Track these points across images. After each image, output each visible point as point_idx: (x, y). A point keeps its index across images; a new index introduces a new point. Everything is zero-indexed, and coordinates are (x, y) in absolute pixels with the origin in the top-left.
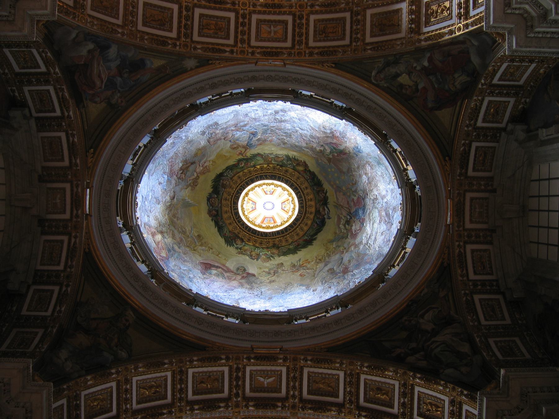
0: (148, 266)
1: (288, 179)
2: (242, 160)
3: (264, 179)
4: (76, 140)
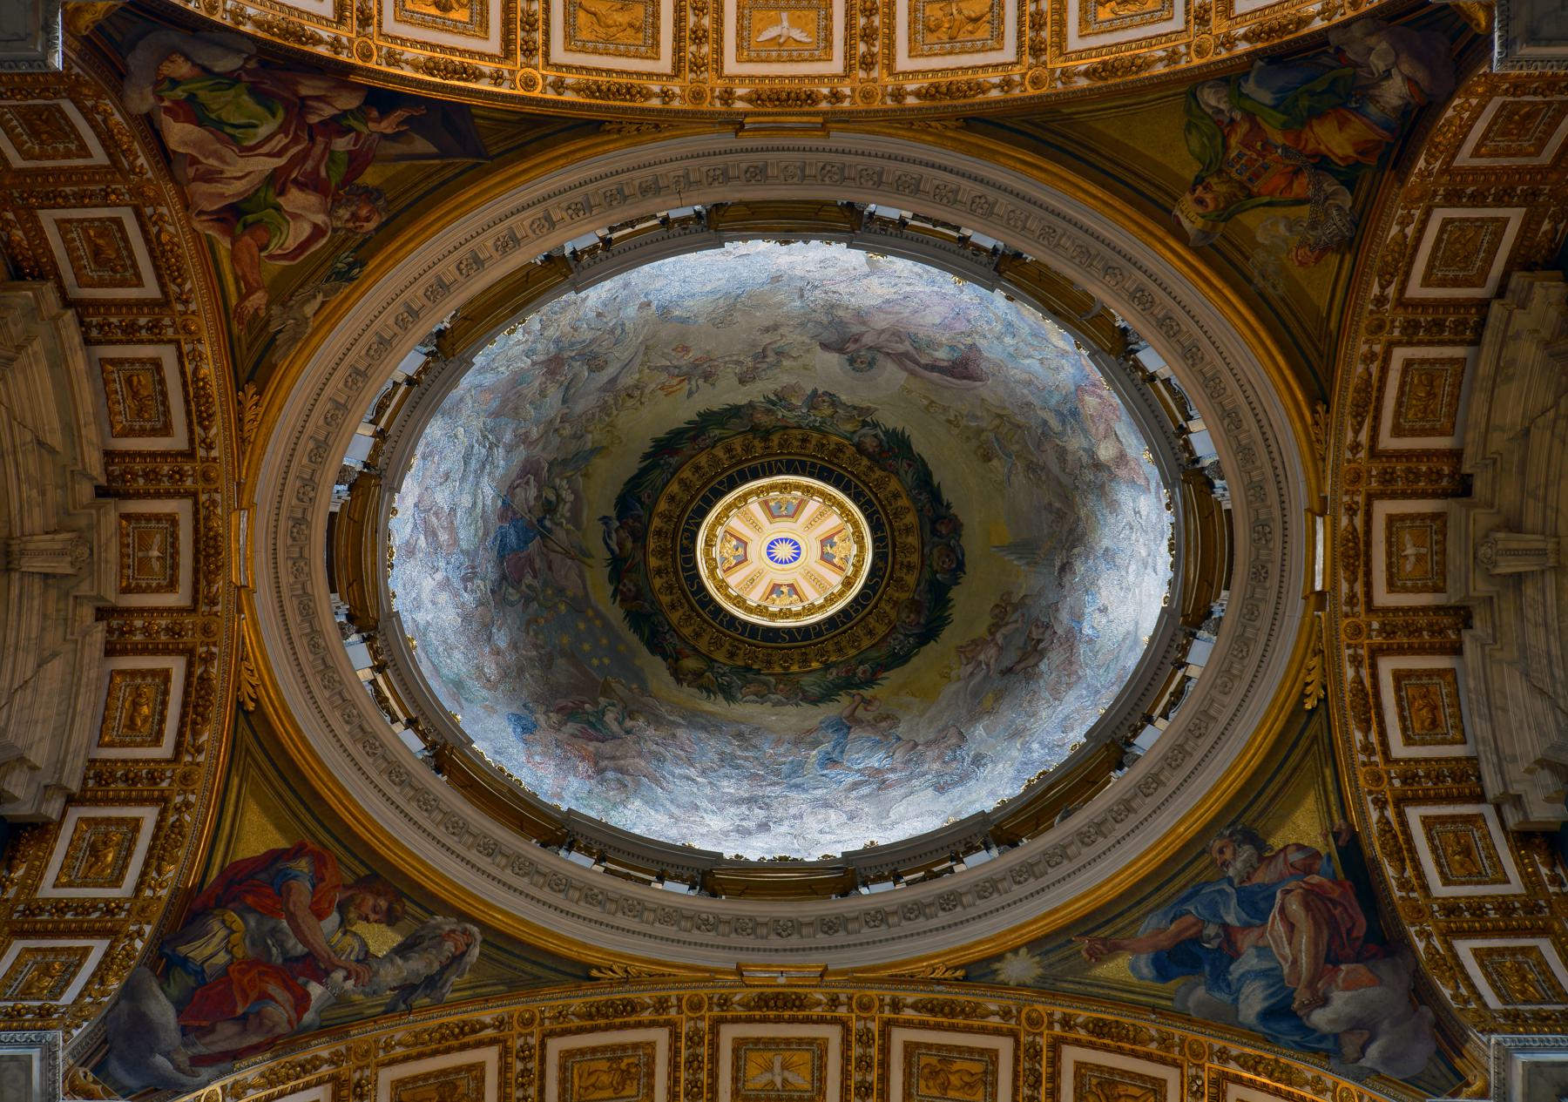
0: (1138, 366)
2: (862, 682)
3: (799, 629)
4: (1358, 736)
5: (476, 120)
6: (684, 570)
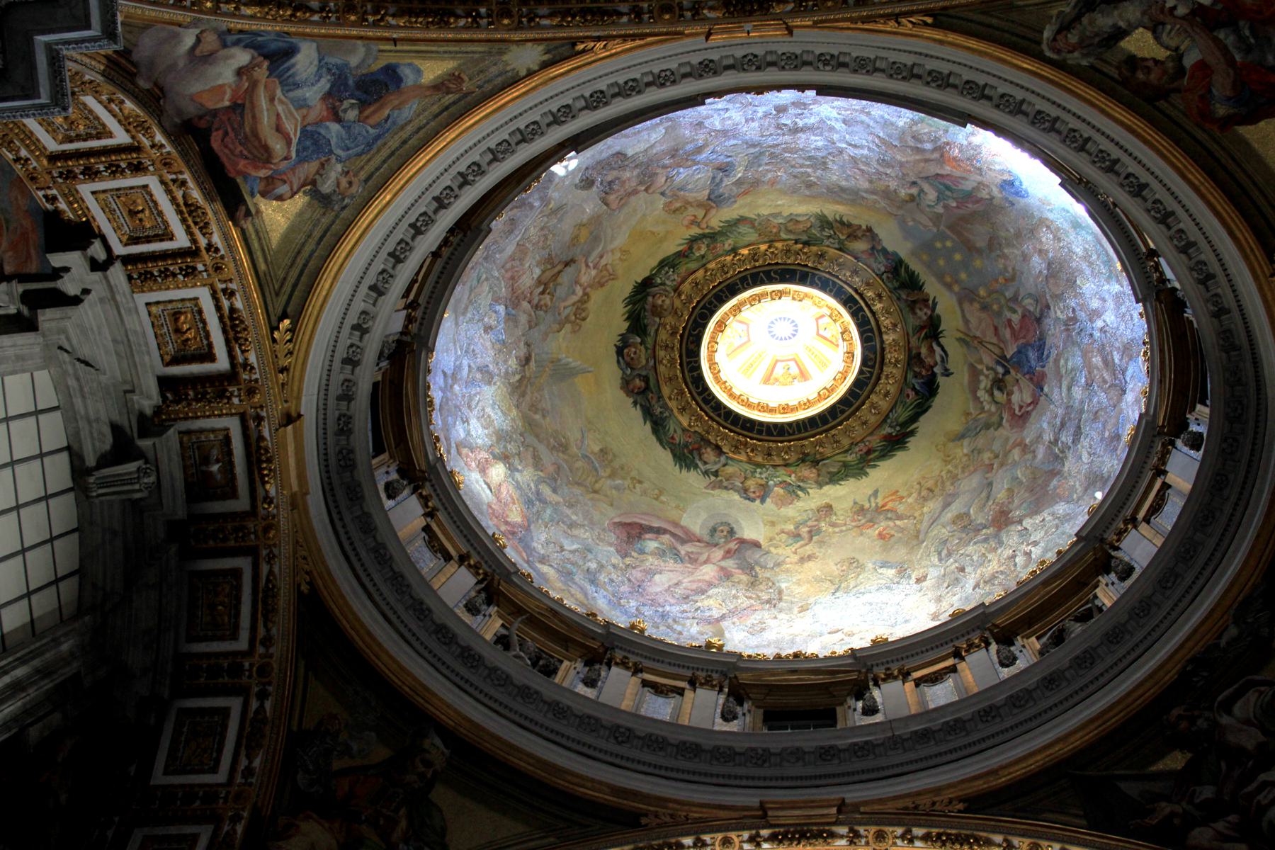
1: (827, 276)
4: (239, 304)
5: (1082, 813)
6: (871, 330)
